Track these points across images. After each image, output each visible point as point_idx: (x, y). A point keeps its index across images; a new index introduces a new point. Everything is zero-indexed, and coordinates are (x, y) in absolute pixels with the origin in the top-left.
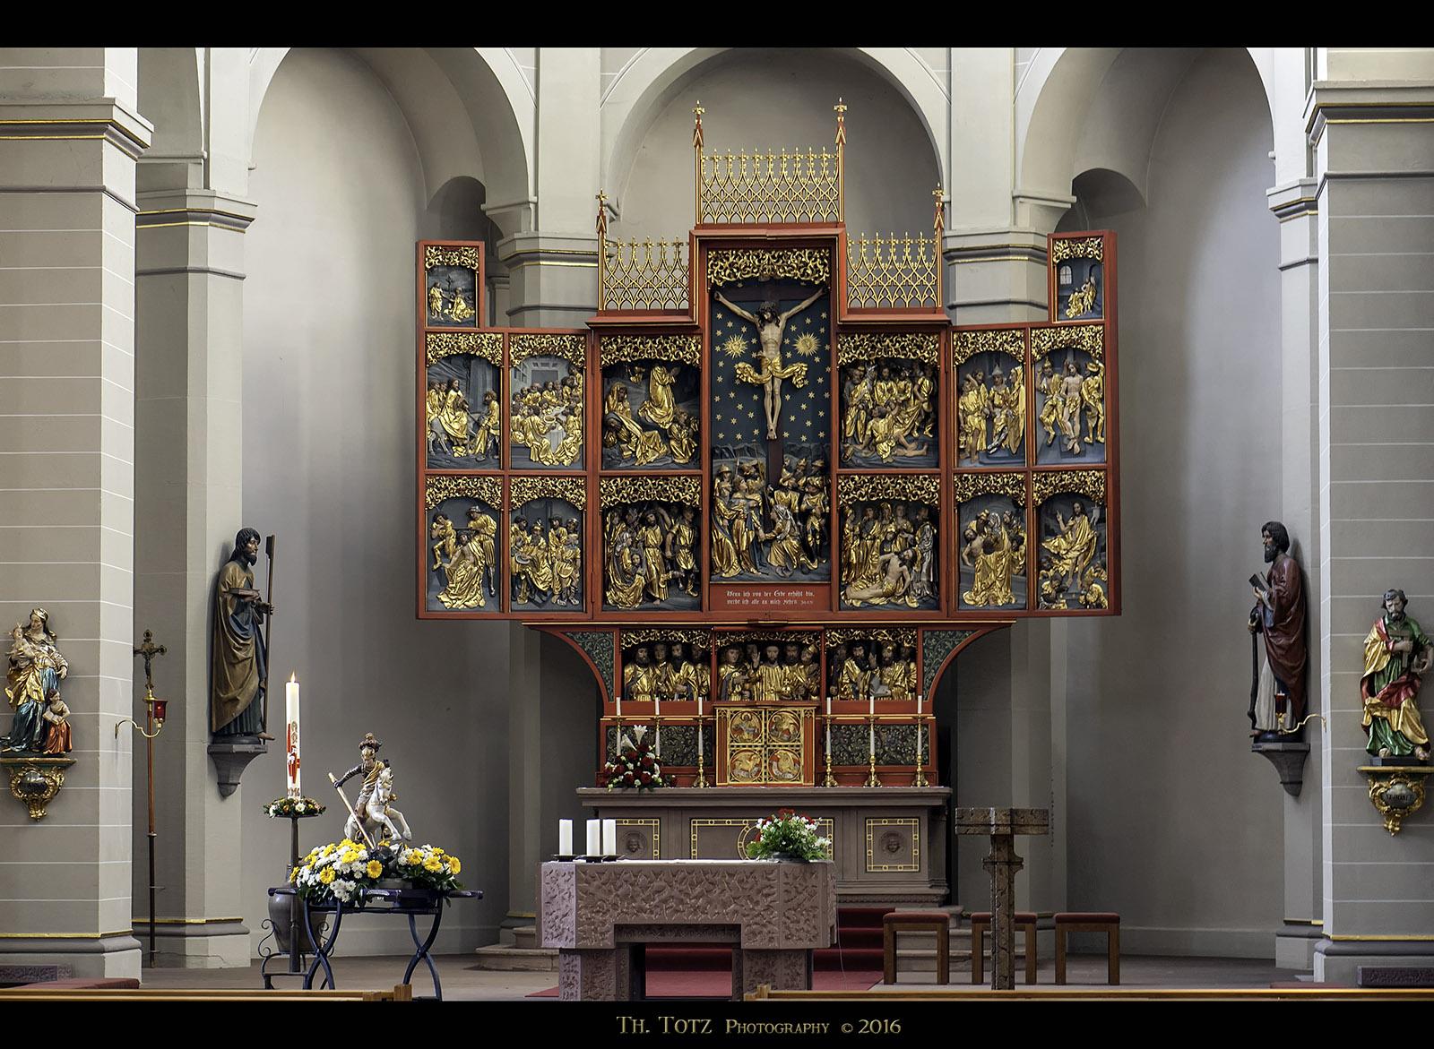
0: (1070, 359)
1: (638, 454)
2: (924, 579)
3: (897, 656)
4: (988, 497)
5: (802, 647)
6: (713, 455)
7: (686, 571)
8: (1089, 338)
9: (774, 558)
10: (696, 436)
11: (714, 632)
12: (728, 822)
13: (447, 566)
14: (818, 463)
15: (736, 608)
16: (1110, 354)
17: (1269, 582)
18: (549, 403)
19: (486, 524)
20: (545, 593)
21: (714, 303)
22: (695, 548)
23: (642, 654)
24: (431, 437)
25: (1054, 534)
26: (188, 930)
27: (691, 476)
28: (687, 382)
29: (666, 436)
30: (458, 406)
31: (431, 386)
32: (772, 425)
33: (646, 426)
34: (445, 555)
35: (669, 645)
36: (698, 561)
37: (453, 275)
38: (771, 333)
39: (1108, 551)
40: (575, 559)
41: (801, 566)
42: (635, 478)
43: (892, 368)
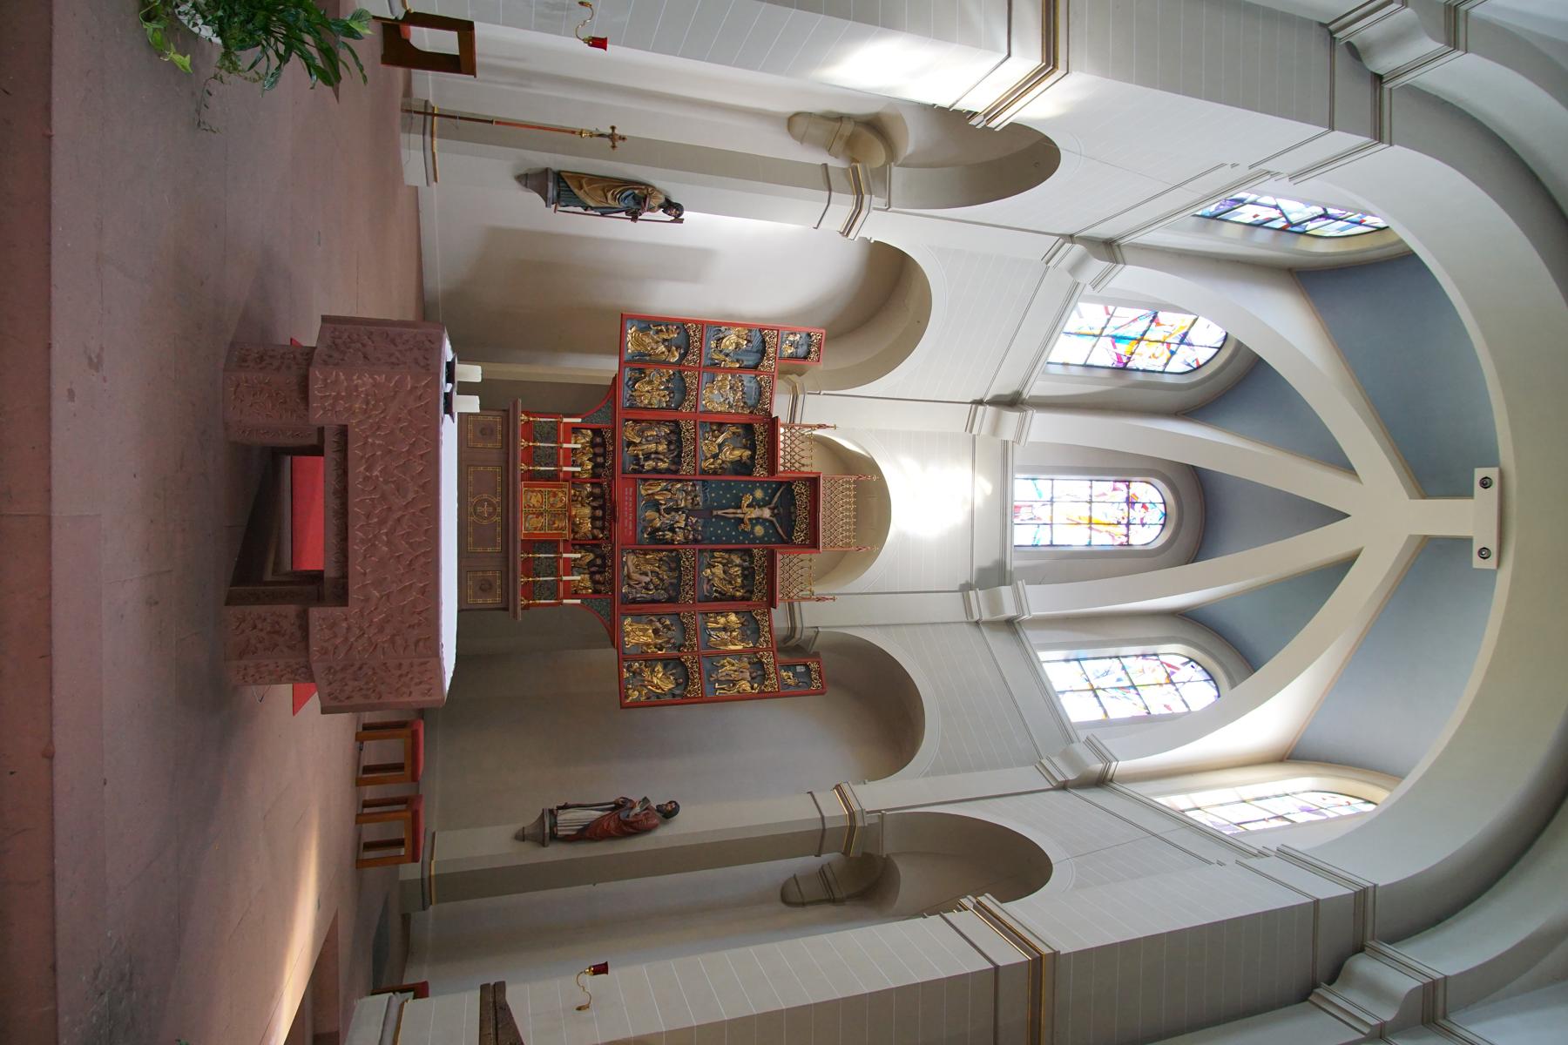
0: (759, 672)
1: (707, 441)
2: (638, 595)
3: (595, 582)
4: (684, 630)
5: (602, 529)
6: (704, 481)
7: (643, 466)
8: (772, 684)
9: (650, 514)
10: (715, 472)
11: (611, 481)
12: (499, 489)
13: (651, 333)
14: (700, 537)
15: (623, 493)
16: (762, 695)
17: (646, 809)
18: (735, 394)
19: (675, 356)
20: (633, 387)
21: (780, 484)
22: (655, 470)
23: (598, 440)
24: (723, 329)
25: (665, 667)
26: (428, 138)
27: (695, 470)
28: (743, 468)
29: (715, 456)
30: (738, 345)
31: (750, 331)
32: (720, 512)
33: (720, 446)
34: (658, 332)
35: (604, 455)
36: (648, 471)
37: (805, 347)
38: (767, 513)
39: (656, 701)
40: (652, 405)
41: (645, 528)
42: (695, 439)
43: (748, 574)
